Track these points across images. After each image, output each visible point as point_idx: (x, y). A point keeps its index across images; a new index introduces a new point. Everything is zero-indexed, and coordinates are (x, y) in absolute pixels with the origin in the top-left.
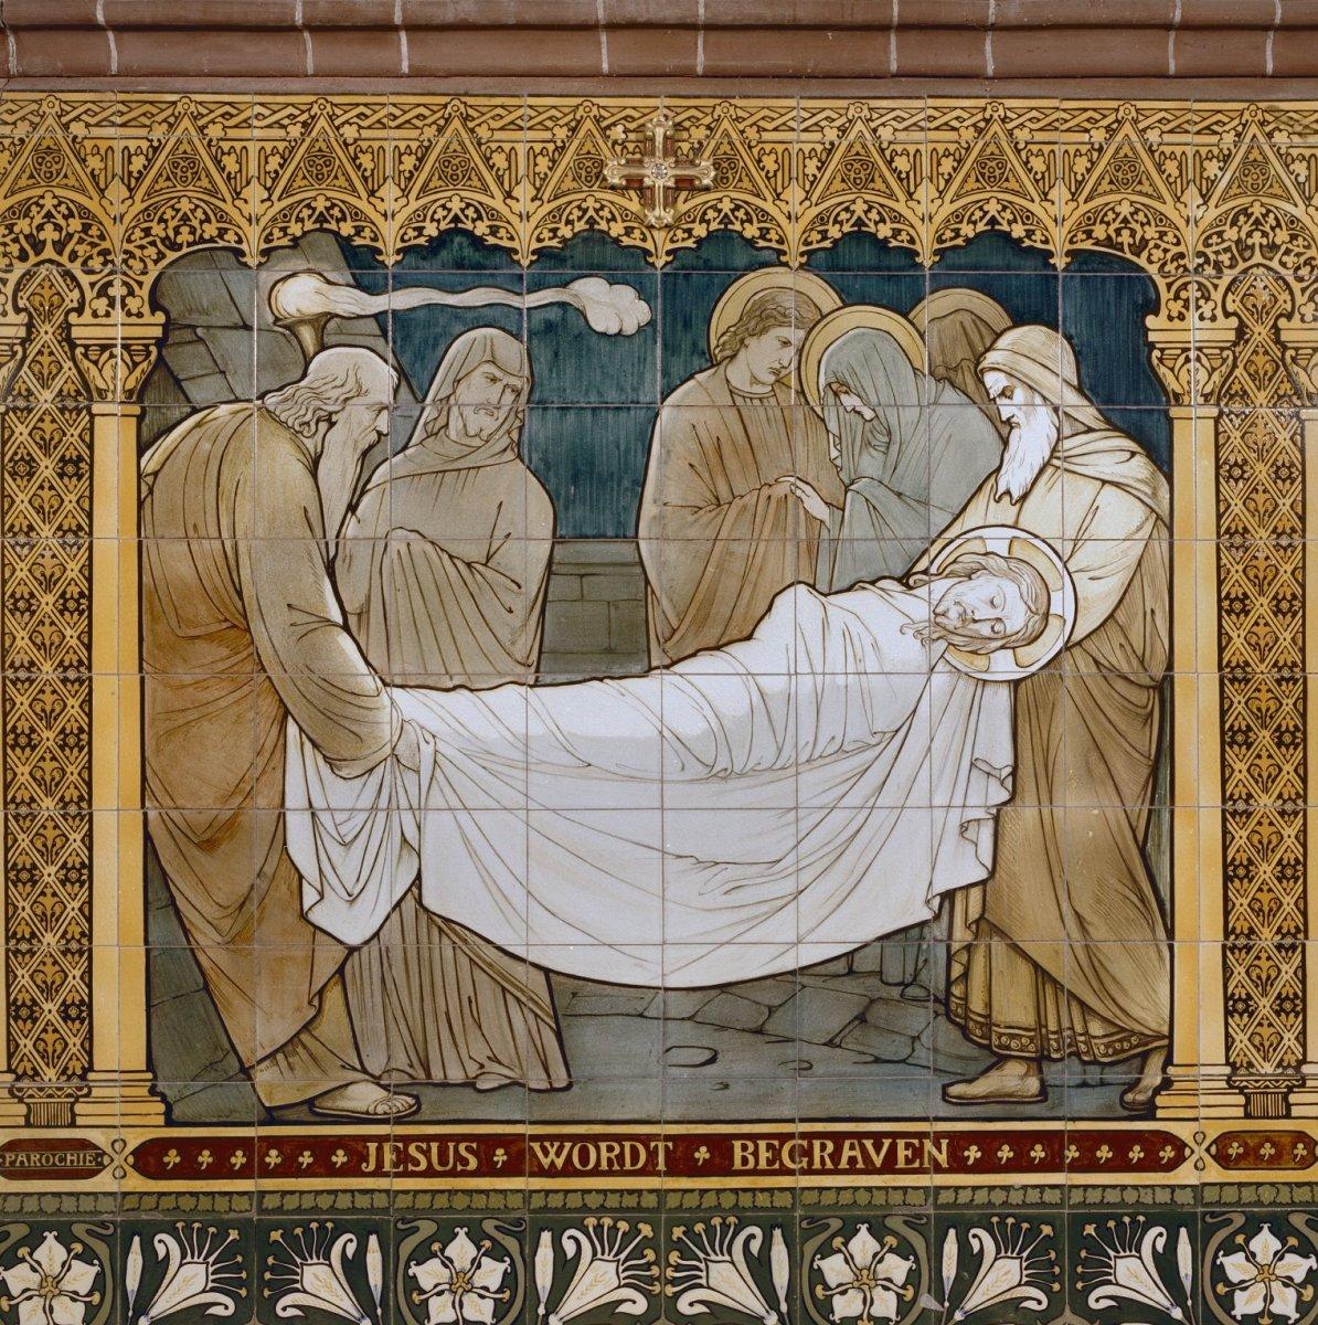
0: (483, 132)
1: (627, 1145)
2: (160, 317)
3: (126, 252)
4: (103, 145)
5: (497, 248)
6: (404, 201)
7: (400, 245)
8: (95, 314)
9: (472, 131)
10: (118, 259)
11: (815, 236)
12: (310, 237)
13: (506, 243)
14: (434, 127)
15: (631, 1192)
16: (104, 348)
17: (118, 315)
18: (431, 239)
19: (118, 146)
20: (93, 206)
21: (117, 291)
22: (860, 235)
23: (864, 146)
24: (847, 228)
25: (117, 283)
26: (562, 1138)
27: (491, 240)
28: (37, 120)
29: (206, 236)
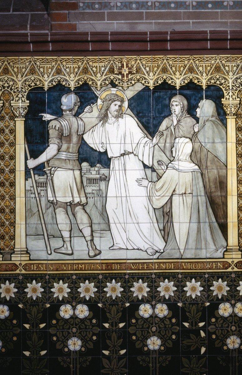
0: (144, 63)
1: (167, 264)
2: (239, 99)
3: (233, 86)
4: (149, 65)
5: (199, 85)
6: (101, 77)
7: (206, 85)
8: (226, 99)
9: (221, 62)
10: (231, 88)
11: (209, 82)
12: (136, 84)
13: (200, 84)
14: (134, 62)
15: (143, 273)
16: (229, 105)
17: (231, 99)
18: (186, 84)
19: (178, 65)
20: (94, 78)
21: (231, 94)
22: (191, 82)
23: (192, 65)
24: (189, 81)
25: (230, 92)
26: (192, 262)
27: (198, 84)
28: (109, 61)
29: (216, 83)
